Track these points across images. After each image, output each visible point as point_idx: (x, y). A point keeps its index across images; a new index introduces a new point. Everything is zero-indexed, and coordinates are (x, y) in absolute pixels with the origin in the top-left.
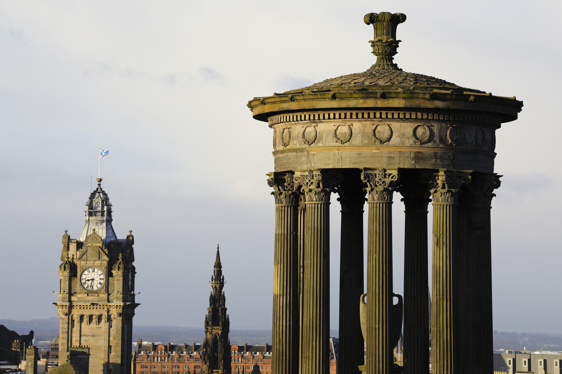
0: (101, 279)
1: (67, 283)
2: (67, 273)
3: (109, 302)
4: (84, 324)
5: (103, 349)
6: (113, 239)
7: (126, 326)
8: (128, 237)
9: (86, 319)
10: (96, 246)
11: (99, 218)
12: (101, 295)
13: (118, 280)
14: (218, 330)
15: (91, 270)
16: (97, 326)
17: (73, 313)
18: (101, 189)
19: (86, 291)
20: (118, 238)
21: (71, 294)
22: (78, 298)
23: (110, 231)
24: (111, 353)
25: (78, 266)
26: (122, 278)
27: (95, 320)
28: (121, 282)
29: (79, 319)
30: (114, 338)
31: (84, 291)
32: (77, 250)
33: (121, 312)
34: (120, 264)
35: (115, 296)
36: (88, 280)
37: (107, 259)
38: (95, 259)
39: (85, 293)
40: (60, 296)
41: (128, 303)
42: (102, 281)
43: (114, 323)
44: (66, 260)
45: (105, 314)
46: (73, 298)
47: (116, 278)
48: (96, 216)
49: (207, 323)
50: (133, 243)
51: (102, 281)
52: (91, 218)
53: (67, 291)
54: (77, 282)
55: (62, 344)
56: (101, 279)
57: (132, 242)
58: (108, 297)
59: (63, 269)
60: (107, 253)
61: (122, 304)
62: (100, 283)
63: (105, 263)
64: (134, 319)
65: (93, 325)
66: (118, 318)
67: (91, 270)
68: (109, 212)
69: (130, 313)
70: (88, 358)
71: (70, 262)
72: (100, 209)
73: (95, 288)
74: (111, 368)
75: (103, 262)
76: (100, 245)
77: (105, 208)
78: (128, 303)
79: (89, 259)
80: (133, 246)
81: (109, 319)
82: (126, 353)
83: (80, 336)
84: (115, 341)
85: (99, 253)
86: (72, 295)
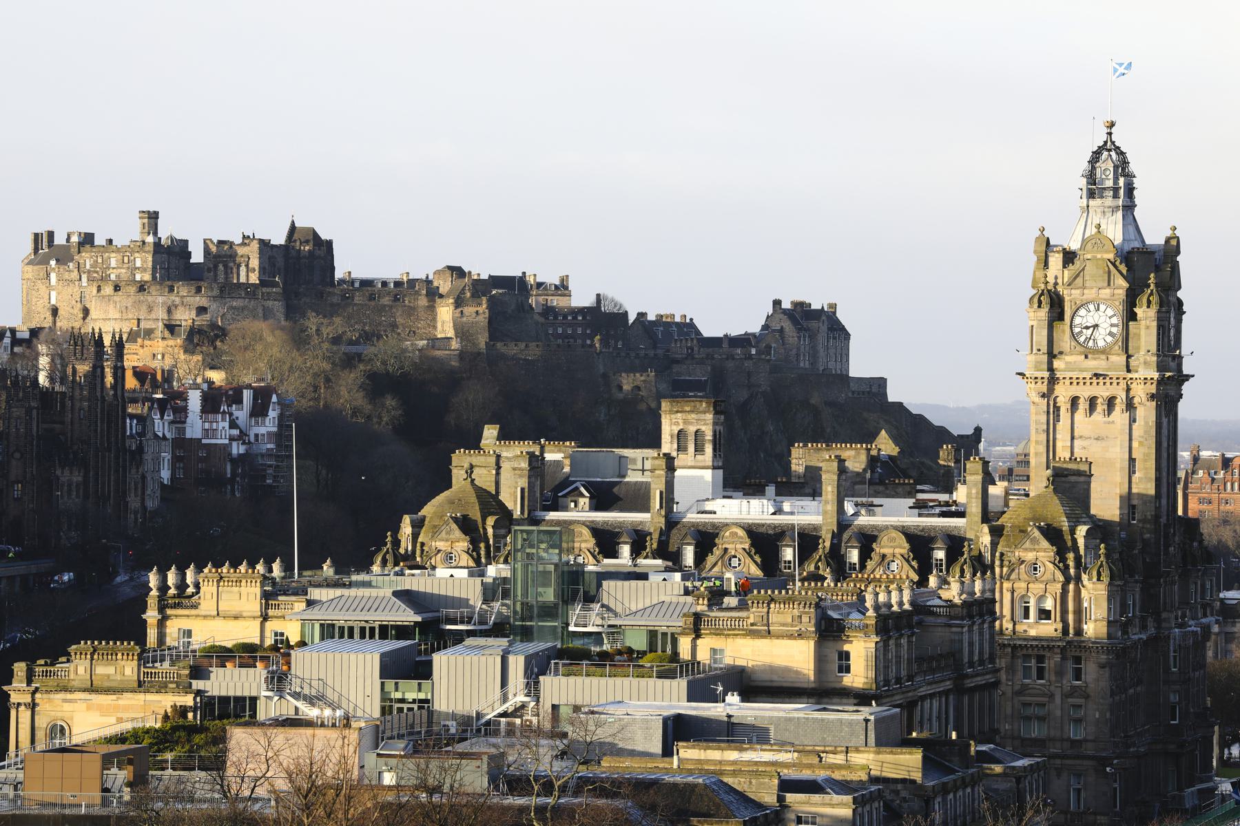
0: (1112, 325)
1: (1045, 332)
2: (1043, 313)
3: (1129, 371)
5: (1118, 465)
6: (1137, 244)
7: (1165, 421)
8: (1168, 240)
9: (1083, 406)
10: (1103, 259)
11: (1109, 201)
13: (1148, 328)
15: (1091, 307)
16: (1106, 419)
17: (1056, 393)
18: (1113, 143)
19: (1082, 349)
21: (1051, 355)
22: (1067, 363)
23: (1131, 229)
24: (1134, 472)
25: (1067, 298)
26: (1155, 324)
27: (1101, 407)
29: (1069, 406)
30: (1141, 443)
31: (1079, 348)
32: (1064, 267)
33: (1154, 391)
34: (1151, 294)
35: (1142, 360)
36: (1087, 328)
37: (1125, 285)
38: (1101, 284)
39: (1081, 353)
40: (1032, 358)
41: (1168, 374)
42: (1114, 330)
43: (1140, 413)
44: (1043, 286)
46: (1057, 364)
47: (1143, 323)
48: (1102, 197)
50: (1178, 253)
51: (1114, 330)
52: (1092, 202)
53: (1045, 349)
54: (1063, 331)
55: (1036, 454)
56: (1112, 325)
57: (1177, 251)
58: (1127, 362)
59: (1036, 305)
60: (1125, 272)
61: (1156, 375)
62: (1111, 334)
63: (1121, 293)
64: (1181, 405)
65: (1098, 416)
66: (1148, 404)
67: (1091, 307)
68: (1130, 190)
69: (1172, 393)
70: (1089, 483)
71: (1049, 291)
72: (1110, 183)
73: (1101, 344)
74: (1135, 502)
75: (1117, 291)
76: (1111, 256)
77: (1121, 181)
78: (1168, 374)
79: (1087, 284)
80: (1178, 259)
81: (1130, 406)
82: (1164, 474)
83: (1073, 438)
84: (1142, 450)
85: (1109, 272)
86: (1055, 357)
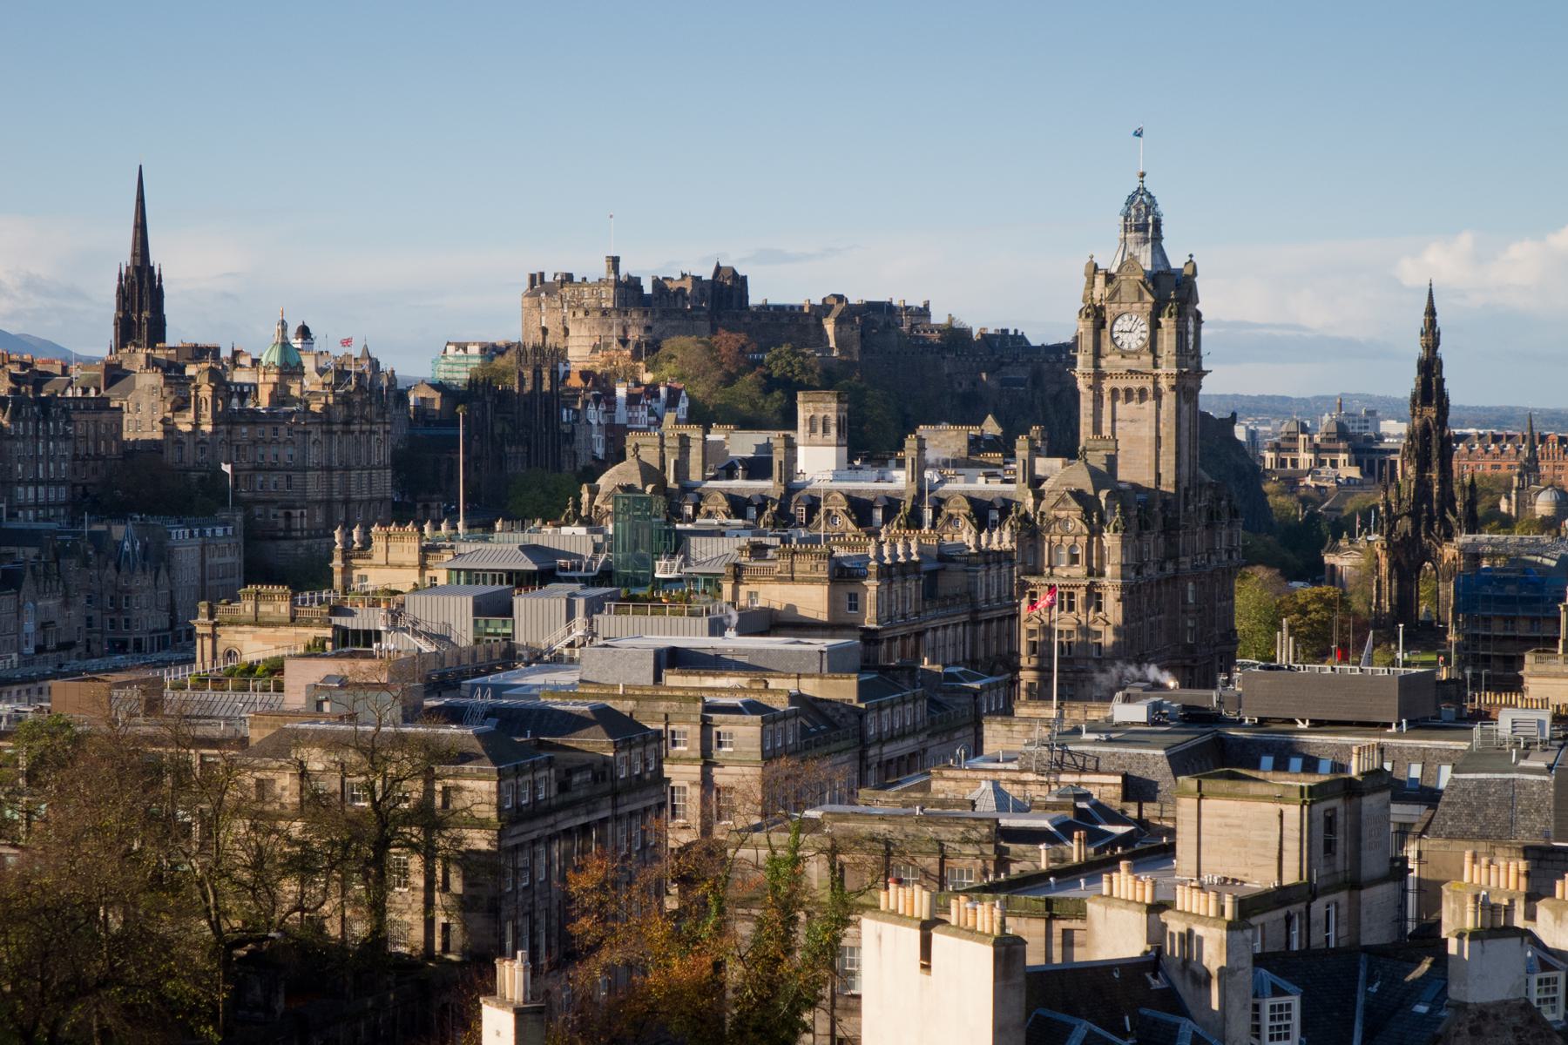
2: (1089, 323)
4: (1118, 404)
7: (1185, 408)
12: (1143, 358)
14: (1431, 412)
20: (1173, 266)
28: (1174, 337)
37: (1151, 299)
42: (1144, 336)
45: (1150, 387)
49: (1414, 400)
53: (1090, 350)
61: (1175, 371)
63: (1149, 307)
65: (1133, 404)
68: (1157, 224)
73: (1134, 347)
81: (1158, 395)
